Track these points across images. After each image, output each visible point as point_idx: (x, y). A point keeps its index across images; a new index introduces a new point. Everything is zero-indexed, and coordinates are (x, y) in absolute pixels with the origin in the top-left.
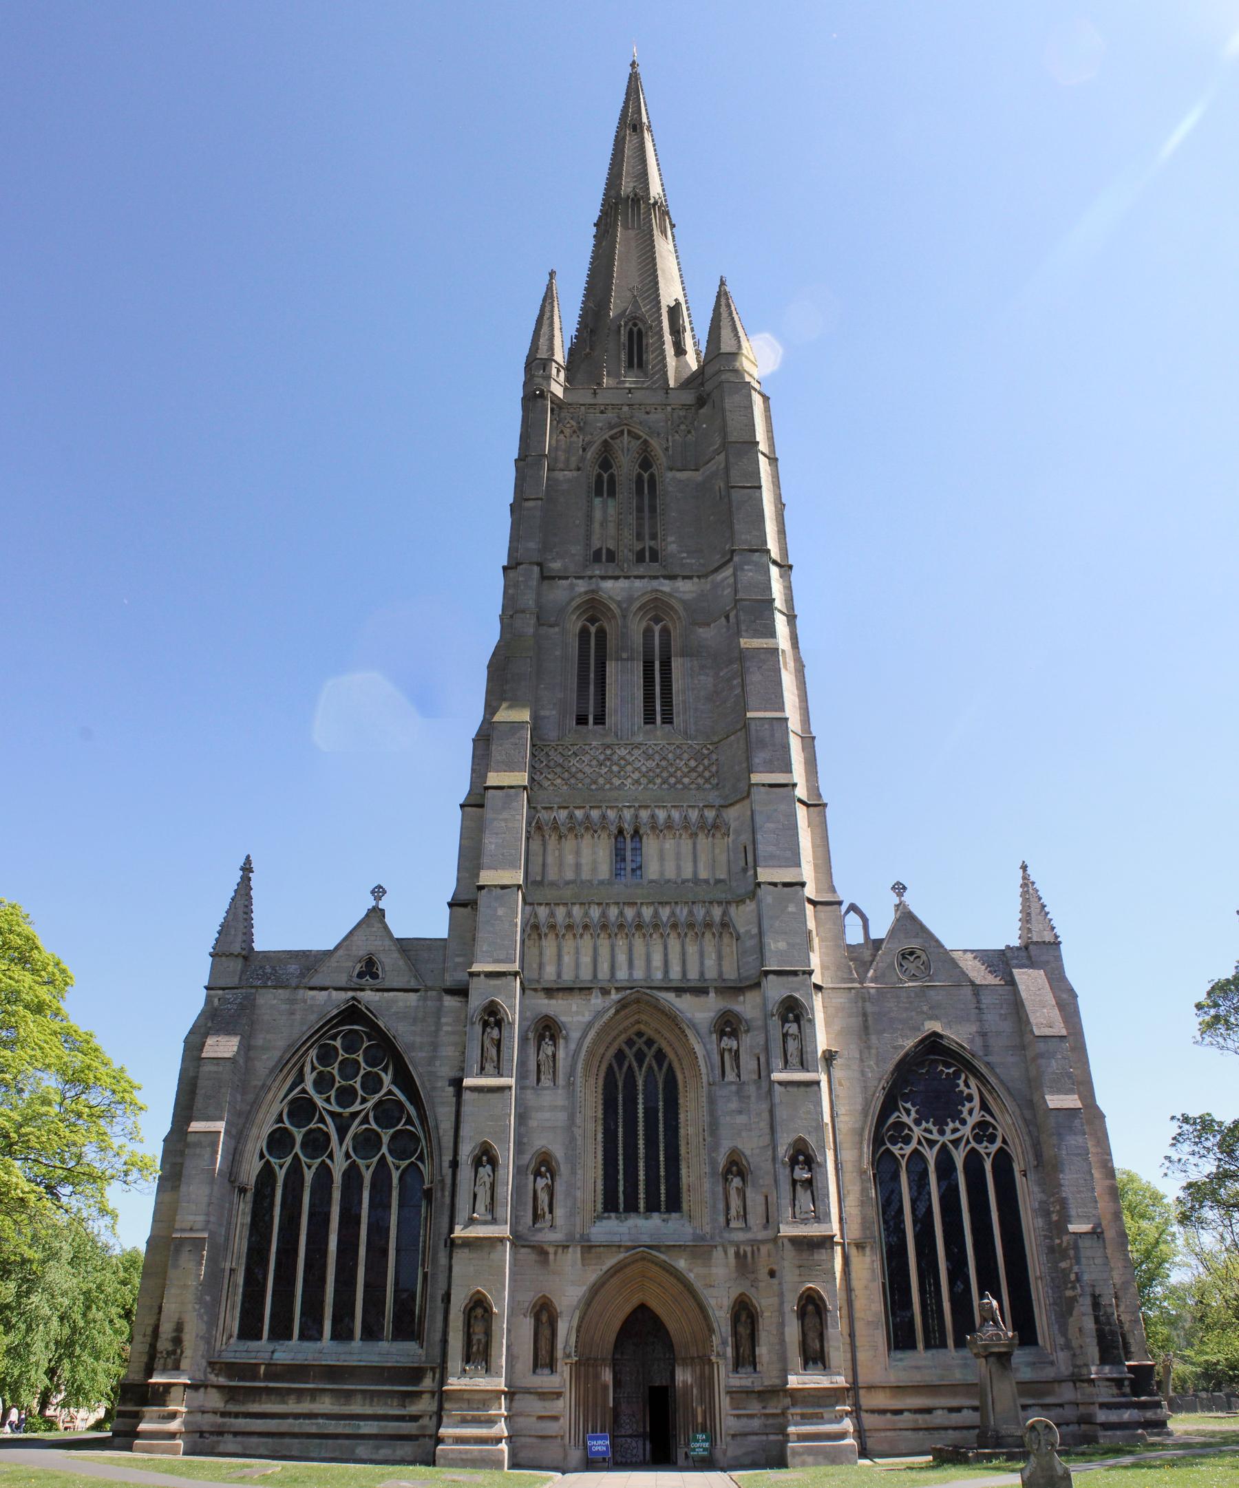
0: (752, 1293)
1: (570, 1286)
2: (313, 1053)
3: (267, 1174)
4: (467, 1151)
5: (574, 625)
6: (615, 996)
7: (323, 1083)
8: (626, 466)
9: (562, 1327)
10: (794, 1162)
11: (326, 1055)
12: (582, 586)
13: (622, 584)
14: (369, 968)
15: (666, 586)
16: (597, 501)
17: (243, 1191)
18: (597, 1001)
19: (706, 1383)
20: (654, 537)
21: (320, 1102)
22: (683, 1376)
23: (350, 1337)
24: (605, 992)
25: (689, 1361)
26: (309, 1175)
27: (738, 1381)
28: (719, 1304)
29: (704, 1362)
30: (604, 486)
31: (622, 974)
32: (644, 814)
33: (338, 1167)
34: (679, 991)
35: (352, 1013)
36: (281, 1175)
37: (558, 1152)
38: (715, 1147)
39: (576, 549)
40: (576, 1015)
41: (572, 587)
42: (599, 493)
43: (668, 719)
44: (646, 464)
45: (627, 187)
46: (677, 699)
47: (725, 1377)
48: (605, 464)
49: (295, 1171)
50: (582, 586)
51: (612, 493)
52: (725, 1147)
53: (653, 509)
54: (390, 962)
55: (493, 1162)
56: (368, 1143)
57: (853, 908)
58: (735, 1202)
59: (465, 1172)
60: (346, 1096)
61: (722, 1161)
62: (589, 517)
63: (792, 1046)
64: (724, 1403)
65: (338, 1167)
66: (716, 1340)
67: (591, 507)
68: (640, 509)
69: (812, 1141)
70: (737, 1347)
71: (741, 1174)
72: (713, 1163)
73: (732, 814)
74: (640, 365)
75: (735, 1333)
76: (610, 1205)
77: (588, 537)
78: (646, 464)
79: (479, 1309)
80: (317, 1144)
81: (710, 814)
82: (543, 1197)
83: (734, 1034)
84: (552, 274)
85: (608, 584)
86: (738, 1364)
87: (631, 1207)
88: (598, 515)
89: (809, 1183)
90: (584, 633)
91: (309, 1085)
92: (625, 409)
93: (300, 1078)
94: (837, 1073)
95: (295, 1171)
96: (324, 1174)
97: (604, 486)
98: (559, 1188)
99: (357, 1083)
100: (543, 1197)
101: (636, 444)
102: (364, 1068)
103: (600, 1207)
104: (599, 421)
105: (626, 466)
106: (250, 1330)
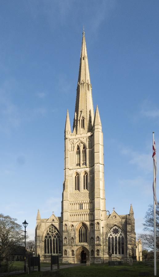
0: (93, 249)
1: (75, 249)
2: (48, 229)
3: (45, 240)
4: (64, 238)
5: (74, 175)
6: (79, 222)
7: (50, 231)
9: (74, 252)
10: (97, 238)
11: (50, 229)
14: (53, 220)
17: (43, 241)
18: (77, 223)
19: (89, 257)
21: (50, 233)
23: (55, 253)
24: (78, 222)
25: (87, 255)
26: (49, 240)
27: (91, 257)
28: (90, 251)
29: (89, 255)
31: (80, 220)
32: (83, 202)
33: (52, 239)
34: (86, 221)
35: (52, 225)
36: (47, 240)
37: (74, 238)
38: (90, 237)
40: (75, 224)
41: (73, 171)
47: (90, 256)
49: (48, 240)
50: (75, 170)
52: (91, 236)
54: (55, 219)
55: (66, 239)
56: (55, 237)
57: (108, 211)
58: (92, 241)
59: (64, 240)
60: (52, 233)
61: (91, 238)
63: (98, 227)
64: (90, 259)
65: (52, 239)
66: (90, 254)
69: (99, 236)
70: (92, 254)
71: (93, 239)
72: (90, 238)
75: (91, 252)
76: (80, 242)
79: (66, 251)
80: (50, 237)
81: (91, 201)
82: (72, 241)
83: (93, 225)
85: (78, 169)
86: (92, 255)
87: (82, 242)
89: (99, 240)
91: (48, 232)
93: (47, 231)
94: (104, 229)
95: (48, 240)
96: (51, 240)
98: (74, 241)
99: (53, 231)
100: (72, 241)
102: (54, 230)
103: (78, 242)
106: (45, 252)
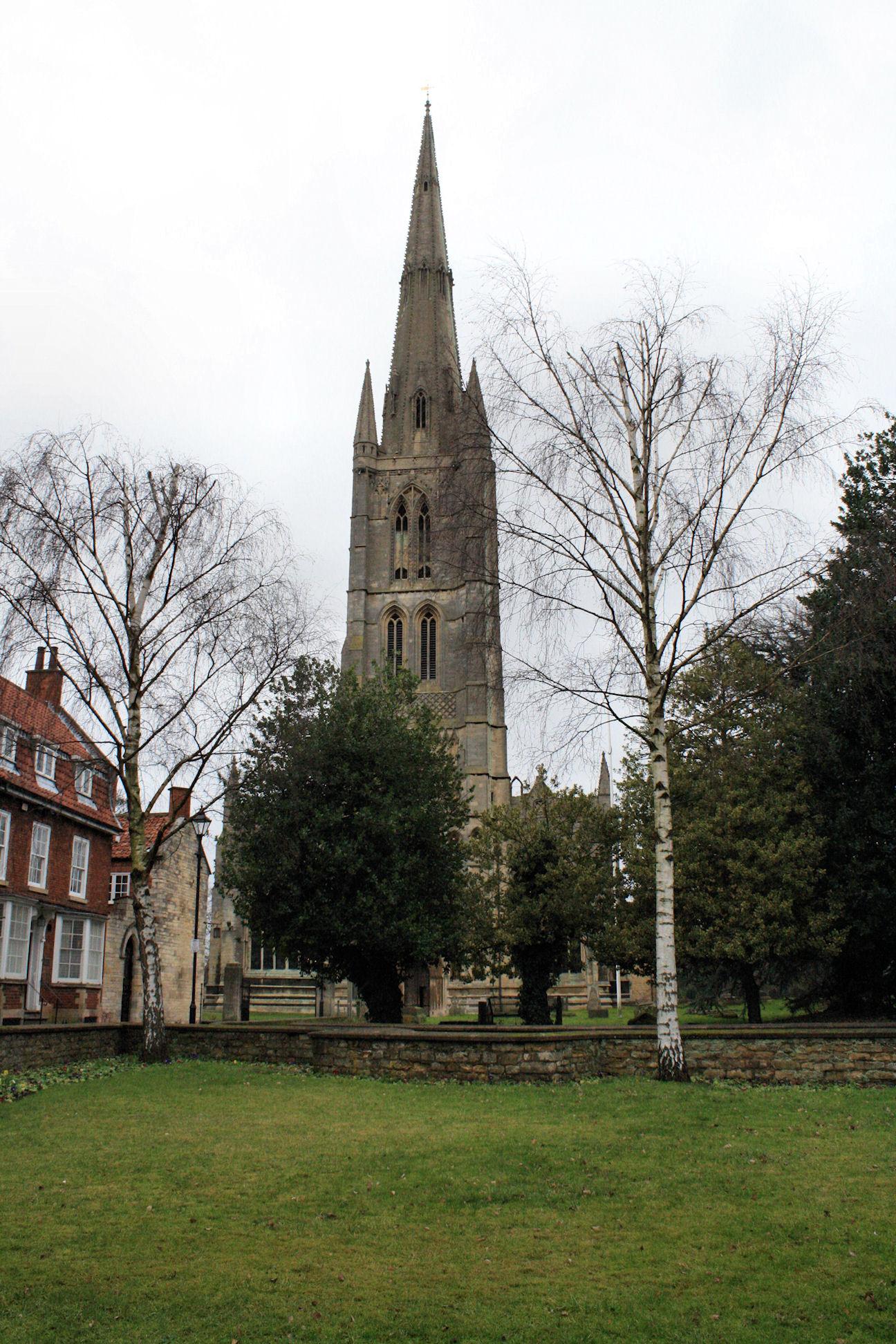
8: (412, 513)
12: (389, 598)
13: (410, 595)
15: (433, 597)
16: (398, 536)
19: (441, 986)
20: (428, 559)
22: (433, 983)
25: (436, 978)
30: (401, 525)
39: (386, 574)
41: (384, 598)
42: (398, 529)
43: (433, 677)
44: (425, 509)
45: (424, 252)
46: (438, 665)
48: (402, 510)
50: (389, 598)
51: (405, 528)
53: (428, 541)
57: (516, 778)
62: (393, 550)
64: (446, 994)
67: (393, 542)
68: (421, 539)
73: (460, 733)
74: (424, 425)
77: (392, 564)
78: (425, 509)
81: (450, 733)
84: (368, 363)
85: (402, 596)
88: (398, 546)
90: (391, 623)
92: (412, 472)
97: (401, 525)
101: (419, 496)
104: (397, 482)
105: (412, 513)
